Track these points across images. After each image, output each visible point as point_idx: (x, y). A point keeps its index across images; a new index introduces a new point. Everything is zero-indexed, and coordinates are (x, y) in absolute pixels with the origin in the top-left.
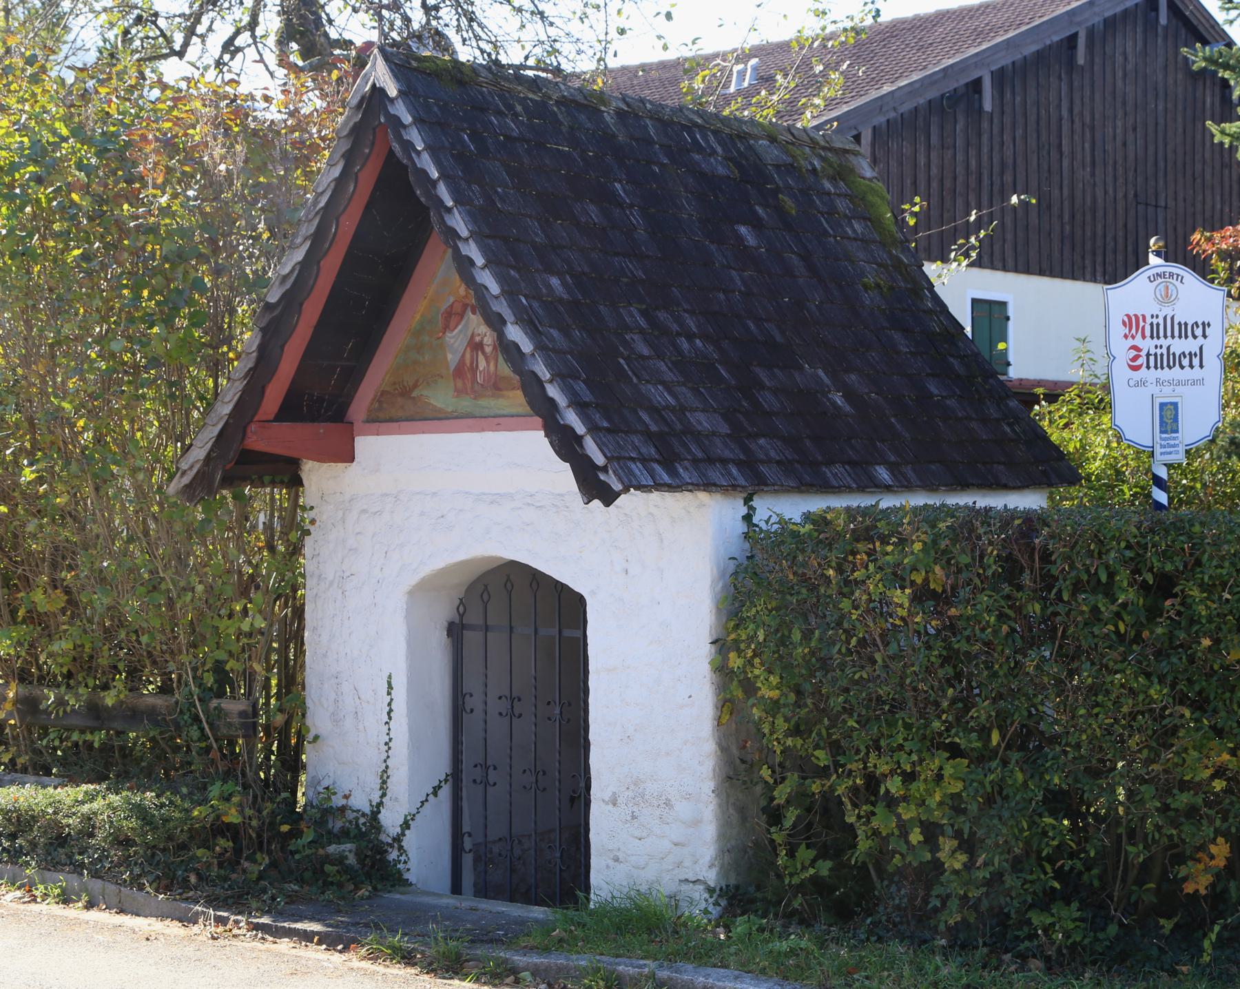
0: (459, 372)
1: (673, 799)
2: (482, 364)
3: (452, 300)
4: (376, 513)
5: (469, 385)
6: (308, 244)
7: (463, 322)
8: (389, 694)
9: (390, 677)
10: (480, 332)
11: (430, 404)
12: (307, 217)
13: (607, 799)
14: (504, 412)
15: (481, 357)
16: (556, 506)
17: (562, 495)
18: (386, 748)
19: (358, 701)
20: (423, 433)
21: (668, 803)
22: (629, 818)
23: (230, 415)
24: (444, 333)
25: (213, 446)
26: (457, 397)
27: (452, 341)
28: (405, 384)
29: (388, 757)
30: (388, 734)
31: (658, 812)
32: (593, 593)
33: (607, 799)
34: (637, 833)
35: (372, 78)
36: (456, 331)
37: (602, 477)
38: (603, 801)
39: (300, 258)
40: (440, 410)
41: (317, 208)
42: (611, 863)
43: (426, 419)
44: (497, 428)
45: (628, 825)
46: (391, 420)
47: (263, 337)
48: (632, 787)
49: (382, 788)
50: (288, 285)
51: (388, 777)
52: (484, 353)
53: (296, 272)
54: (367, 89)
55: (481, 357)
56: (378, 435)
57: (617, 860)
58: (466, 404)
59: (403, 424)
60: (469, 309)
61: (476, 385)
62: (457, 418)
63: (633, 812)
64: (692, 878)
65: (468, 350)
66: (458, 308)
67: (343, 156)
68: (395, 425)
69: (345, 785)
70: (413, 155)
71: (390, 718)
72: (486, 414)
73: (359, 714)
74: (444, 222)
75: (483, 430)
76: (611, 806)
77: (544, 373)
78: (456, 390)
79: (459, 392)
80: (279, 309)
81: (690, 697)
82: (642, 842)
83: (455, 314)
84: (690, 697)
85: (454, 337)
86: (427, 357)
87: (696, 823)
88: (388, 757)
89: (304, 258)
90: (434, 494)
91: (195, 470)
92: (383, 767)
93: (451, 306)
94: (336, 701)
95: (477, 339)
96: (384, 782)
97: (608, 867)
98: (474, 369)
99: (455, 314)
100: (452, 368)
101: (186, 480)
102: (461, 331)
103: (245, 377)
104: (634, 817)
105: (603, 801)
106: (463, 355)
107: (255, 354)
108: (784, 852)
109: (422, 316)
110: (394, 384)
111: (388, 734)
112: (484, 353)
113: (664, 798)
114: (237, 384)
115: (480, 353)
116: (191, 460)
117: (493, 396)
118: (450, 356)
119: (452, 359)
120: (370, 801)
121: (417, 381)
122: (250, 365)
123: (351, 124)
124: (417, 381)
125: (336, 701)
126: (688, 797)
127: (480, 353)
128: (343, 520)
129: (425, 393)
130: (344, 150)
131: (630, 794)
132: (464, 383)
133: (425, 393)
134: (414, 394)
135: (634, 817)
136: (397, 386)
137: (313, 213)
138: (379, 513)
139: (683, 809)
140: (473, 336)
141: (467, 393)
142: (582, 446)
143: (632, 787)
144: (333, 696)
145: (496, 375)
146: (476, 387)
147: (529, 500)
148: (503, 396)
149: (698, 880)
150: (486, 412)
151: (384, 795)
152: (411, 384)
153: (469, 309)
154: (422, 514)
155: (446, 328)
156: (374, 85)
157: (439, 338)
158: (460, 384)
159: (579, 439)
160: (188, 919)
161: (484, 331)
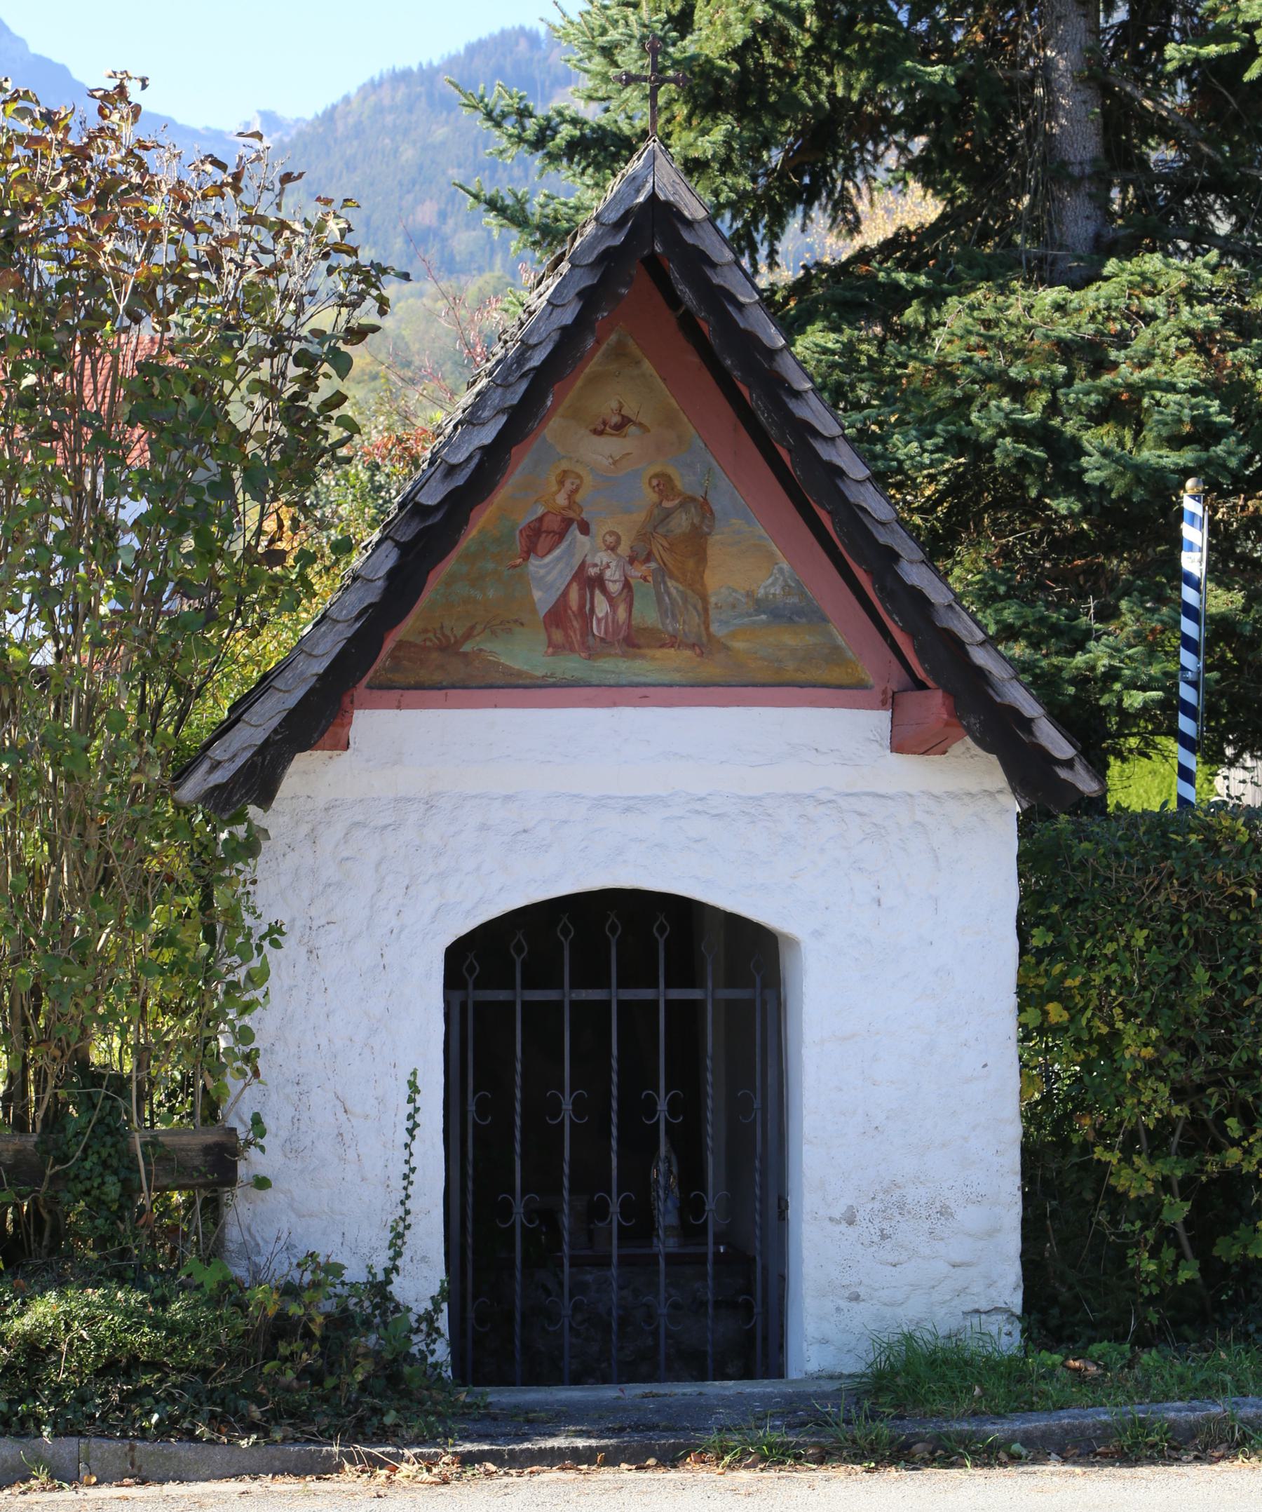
0: (557, 616)
1: (953, 1205)
2: (602, 607)
3: (540, 510)
4: (385, 827)
5: (576, 638)
6: (503, 419)
7: (564, 545)
8: (411, 1100)
9: (414, 1073)
10: (597, 561)
11: (498, 664)
12: (505, 379)
13: (838, 1216)
14: (642, 679)
15: (599, 598)
16: (748, 814)
17: (759, 799)
18: (405, 1183)
19: (342, 1117)
20: (496, 706)
21: (945, 1212)
22: (876, 1239)
23: (321, 678)
24: (526, 559)
25: (284, 720)
26: (553, 654)
27: (542, 572)
28: (448, 632)
29: (408, 1197)
30: (407, 1162)
31: (927, 1225)
32: (817, 934)
33: (838, 1216)
34: (892, 1258)
35: (649, 186)
36: (548, 559)
37: (1063, 774)
38: (831, 1219)
39: (487, 441)
40: (520, 674)
41: (526, 368)
42: (843, 1304)
43: (491, 687)
44: (644, 701)
45: (875, 1248)
46: (419, 686)
47: (401, 557)
48: (880, 1196)
49: (392, 1245)
50: (460, 479)
51: (408, 1227)
52: (604, 591)
53: (475, 461)
54: (641, 199)
55: (599, 598)
56: (399, 707)
57: (856, 1298)
58: (572, 665)
59: (451, 692)
60: (575, 526)
61: (590, 638)
62: (554, 686)
63: (882, 1230)
64: (984, 1306)
65: (575, 587)
66: (553, 523)
67: (580, 295)
68: (396, 694)
69: (329, 1248)
70: (730, 308)
71: (413, 1137)
72: (612, 682)
73: (347, 1137)
74: (790, 415)
75: (615, 704)
76: (844, 1226)
77: (971, 634)
78: (550, 644)
79: (556, 648)
80: (439, 516)
81: (985, 1066)
82: (899, 1268)
83: (548, 532)
84: (985, 1066)
85: (546, 565)
86: (491, 594)
87: (992, 1233)
88: (408, 1197)
89: (494, 441)
90: (508, 798)
91: (239, 762)
92: (400, 1211)
93: (541, 519)
94: (295, 1120)
95: (592, 571)
96: (400, 1236)
97: (838, 1309)
98: (586, 615)
99: (548, 532)
100: (542, 612)
101: (220, 777)
102: (559, 559)
103: (357, 618)
104: (884, 1237)
105: (831, 1219)
106: (565, 594)
107: (380, 583)
108: (1147, 1255)
109: (480, 532)
110: (426, 631)
111: (407, 1162)
112: (604, 591)
113: (938, 1204)
114: (340, 627)
115: (597, 592)
116: (235, 746)
117: (624, 655)
118: (537, 595)
119: (543, 599)
120: (370, 1268)
121: (473, 628)
122: (372, 598)
123: (601, 248)
124: (473, 628)
125: (295, 1120)
126: (979, 1200)
127: (597, 592)
128: (313, 837)
129: (487, 646)
130: (583, 286)
131: (877, 1205)
132: (567, 636)
133: (487, 646)
134: (466, 648)
135: (884, 1237)
136: (431, 635)
137: (518, 374)
138: (397, 826)
139: (969, 1217)
140: (583, 566)
141: (572, 650)
142: (1030, 732)
143: (880, 1196)
144: (289, 1112)
145: (629, 626)
146: (591, 640)
147: (698, 806)
148: (643, 657)
149: (996, 1309)
150: (612, 679)
151: (398, 1254)
152: (459, 632)
153: (575, 526)
154: (484, 827)
155: (530, 550)
156: (653, 197)
157: (515, 567)
158: (558, 636)
159: (1027, 724)
160: (324, 1469)
161: (605, 560)
